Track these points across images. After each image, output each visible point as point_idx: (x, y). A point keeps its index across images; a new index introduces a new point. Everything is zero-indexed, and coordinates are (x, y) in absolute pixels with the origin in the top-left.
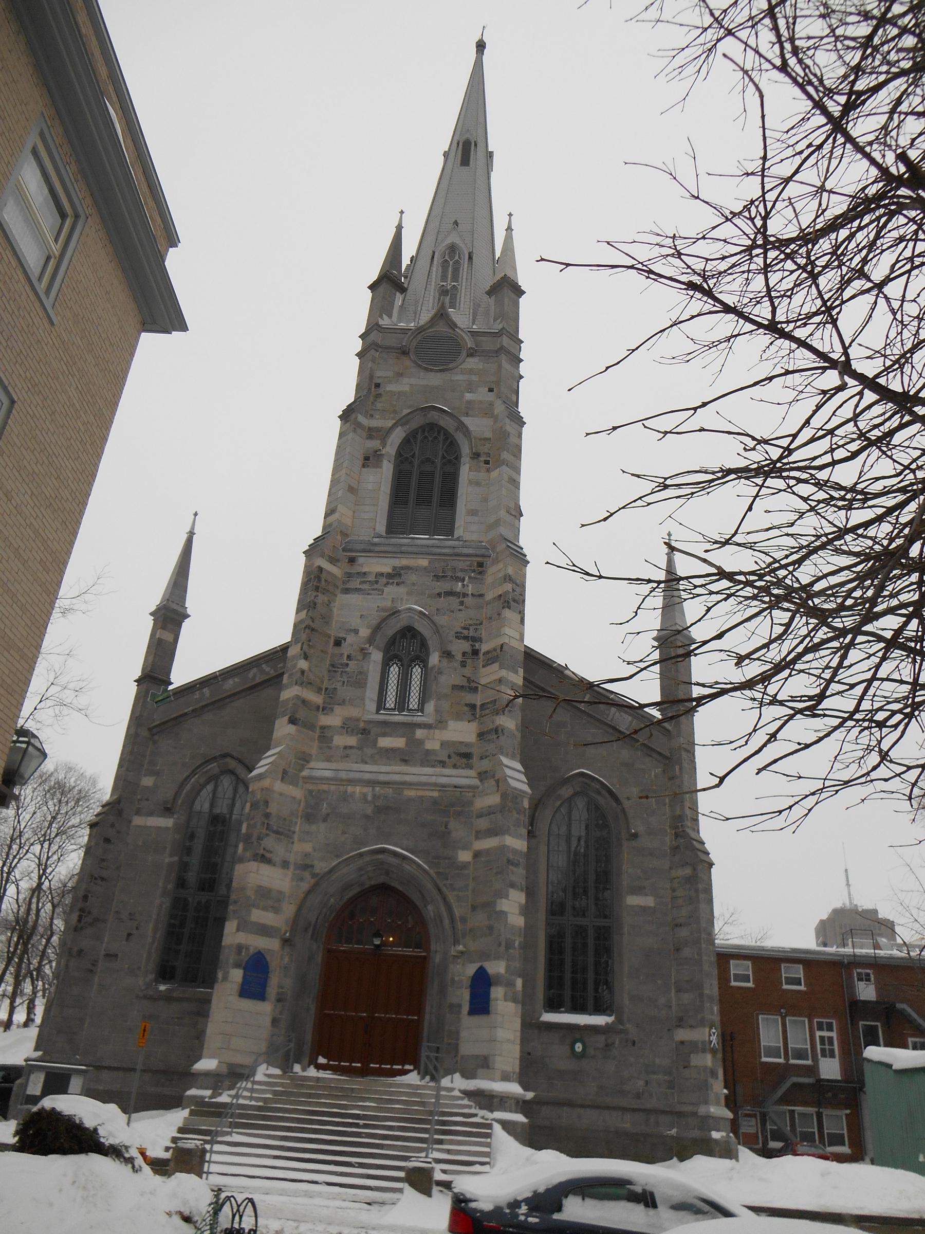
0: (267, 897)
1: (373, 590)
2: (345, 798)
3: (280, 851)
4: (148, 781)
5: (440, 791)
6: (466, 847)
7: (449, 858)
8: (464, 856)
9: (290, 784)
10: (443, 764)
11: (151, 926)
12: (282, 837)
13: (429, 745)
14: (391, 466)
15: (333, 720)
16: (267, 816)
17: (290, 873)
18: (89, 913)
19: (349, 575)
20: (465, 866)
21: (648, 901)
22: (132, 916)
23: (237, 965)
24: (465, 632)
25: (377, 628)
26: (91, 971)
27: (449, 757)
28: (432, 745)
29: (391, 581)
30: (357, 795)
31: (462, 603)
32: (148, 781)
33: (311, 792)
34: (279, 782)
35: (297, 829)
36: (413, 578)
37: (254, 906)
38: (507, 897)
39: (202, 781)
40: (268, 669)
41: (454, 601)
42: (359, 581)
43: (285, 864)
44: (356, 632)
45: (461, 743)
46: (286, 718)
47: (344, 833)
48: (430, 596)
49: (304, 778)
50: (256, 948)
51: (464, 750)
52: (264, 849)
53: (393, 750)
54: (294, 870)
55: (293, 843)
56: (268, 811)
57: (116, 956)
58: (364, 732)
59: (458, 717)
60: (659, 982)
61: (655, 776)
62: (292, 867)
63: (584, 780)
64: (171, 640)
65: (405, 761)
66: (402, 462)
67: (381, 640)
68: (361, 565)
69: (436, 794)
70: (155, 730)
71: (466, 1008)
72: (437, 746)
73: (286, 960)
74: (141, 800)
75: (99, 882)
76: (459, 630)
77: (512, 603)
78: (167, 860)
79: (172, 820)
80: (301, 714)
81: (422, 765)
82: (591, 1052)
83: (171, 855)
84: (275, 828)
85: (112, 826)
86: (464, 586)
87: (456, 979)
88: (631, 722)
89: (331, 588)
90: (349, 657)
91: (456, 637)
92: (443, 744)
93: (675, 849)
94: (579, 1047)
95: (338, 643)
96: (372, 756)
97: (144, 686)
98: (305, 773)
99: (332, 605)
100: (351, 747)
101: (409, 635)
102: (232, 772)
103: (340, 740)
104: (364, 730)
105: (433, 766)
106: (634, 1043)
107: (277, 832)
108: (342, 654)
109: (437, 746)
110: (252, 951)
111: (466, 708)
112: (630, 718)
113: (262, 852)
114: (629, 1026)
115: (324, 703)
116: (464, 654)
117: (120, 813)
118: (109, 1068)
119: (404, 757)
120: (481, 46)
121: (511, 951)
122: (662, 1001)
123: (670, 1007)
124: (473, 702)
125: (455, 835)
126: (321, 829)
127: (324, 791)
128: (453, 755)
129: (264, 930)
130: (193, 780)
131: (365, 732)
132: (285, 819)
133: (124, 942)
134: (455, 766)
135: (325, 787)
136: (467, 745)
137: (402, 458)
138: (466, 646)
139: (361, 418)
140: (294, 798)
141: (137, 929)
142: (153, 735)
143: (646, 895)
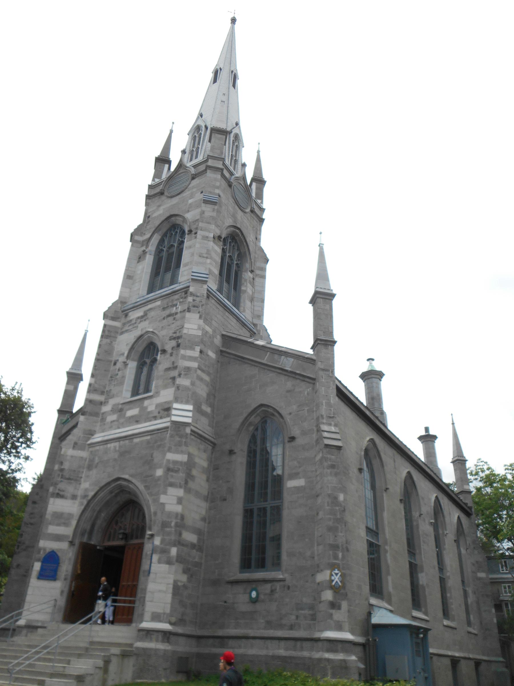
0: (61, 518)
3: (70, 489)
5: (150, 435)
7: (151, 476)
9: (79, 449)
10: (155, 418)
12: (72, 481)
13: (149, 409)
14: (152, 257)
15: (106, 409)
16: (62, 470)
17: (77, 502)
18: (24, 543)
19: (124, 324)
20: (159, 478)
25: (132, 348)
26: (25, 576)
31: (174, 319)
33: (91, 452)
35: (83, 476)
36: (152, 314)
37: (50, 524)
38: (165, 493)
41: (171, 318)
42: (128, 325)
43: (74, 497)
45: (165, 402)
47: (104, 472)
48: (160, 321)
49: (89, 445)
52: (59, 490)
53: (132, 417)
55: (80, 484)
56: (62, 467)
58: (121, 410)
59: (165, 387)
61: (308, 394)
62: (79, 498)
63: (263, 408)
65: (137, 422)
68: (130, 317)
76: (171, 335)
77: (192, 308)
81: (145, 422)
82: (262, 597)
84: (67, 477)
85: (37, 494)
86: (176, 308)
88: (293, 362)
89: (113, 334)
90: (119, 370)
92: (157, 406)
94: (254, 594)
96: (123, 423)
98: (89, 442)
99: (114, 343)
100: (114, 421)
101: (152, 347)
103: (110, 418)
105: (150, 421)
106: (289, 588)
107: (69, 479)
108: (116, 369)
110: (48, 551)
111: (170, 380)
112: (292, 360)
113: (57, 491)
115: (105, 399)
119: (136, 420)
120: (234, 21)
121: (168, 529)
122: (308, 553)
123: (314, 557)
125: (156, 461)
126: (94, 472)
129: (58, 538)
131: (120, 410)
132: (74, 471)
134: (161, 418)
137: (159, 251)
138: (173, 343)
139: (137, 238)
140: (82, 458)
143: (300, 478)
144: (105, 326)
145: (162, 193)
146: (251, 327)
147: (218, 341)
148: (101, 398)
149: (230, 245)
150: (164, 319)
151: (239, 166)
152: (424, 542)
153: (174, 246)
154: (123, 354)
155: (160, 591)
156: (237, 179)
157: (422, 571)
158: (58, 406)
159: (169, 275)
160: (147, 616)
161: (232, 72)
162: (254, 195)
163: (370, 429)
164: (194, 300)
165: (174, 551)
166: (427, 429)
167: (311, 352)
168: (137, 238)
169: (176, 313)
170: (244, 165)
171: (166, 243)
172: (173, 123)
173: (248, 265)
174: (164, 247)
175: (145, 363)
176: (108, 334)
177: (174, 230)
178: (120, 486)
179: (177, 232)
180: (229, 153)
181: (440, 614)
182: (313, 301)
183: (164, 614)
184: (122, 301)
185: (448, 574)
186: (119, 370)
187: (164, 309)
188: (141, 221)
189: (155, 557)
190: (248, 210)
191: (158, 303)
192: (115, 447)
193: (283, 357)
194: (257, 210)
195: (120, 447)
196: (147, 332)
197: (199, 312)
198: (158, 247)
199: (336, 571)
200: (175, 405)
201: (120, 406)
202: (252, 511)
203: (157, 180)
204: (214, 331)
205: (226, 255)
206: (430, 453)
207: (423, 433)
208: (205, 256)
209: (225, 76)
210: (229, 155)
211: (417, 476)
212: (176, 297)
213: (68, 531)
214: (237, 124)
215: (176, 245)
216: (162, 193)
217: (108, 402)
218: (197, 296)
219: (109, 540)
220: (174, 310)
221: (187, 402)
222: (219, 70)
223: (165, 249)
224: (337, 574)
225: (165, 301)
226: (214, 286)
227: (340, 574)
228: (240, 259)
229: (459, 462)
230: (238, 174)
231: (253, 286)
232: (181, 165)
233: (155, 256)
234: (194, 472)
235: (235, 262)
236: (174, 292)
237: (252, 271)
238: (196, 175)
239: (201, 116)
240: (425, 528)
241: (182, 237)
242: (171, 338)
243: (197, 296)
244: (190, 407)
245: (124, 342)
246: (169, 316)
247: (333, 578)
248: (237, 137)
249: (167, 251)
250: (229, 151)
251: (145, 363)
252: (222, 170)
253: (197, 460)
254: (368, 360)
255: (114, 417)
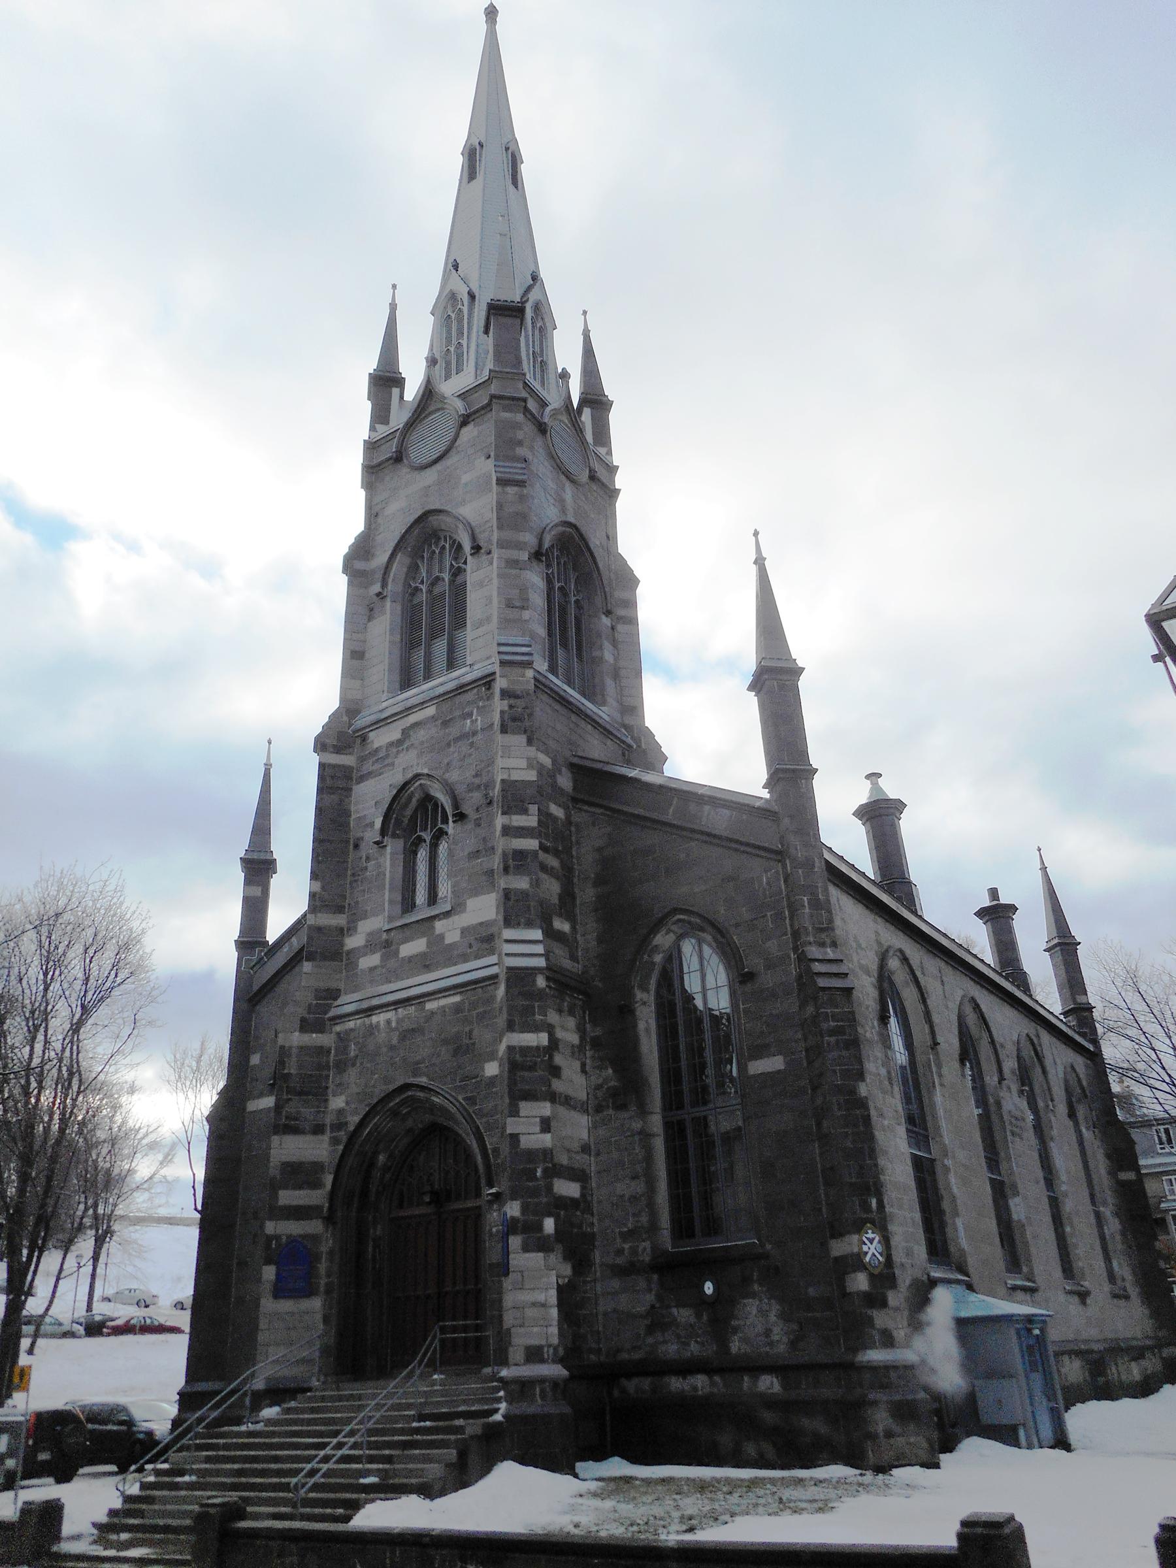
0: (300, 1174)
2: (371, 1030)
5: (461, 993)
6: (492, 1056)
10: (465, 958)
15: (353, 942)
17: (326, 1138)
19: (362, 759)
20: (492, 1080)
21: (773, 1064)
28: (452, 937)
30: (382, 1023)
34: (297, 1034)
36: (421, 735)
38: (515, 1113)
43: (318, 1130)
45: (481, 924)
49: (331, 1019)
50: (289, 1236)
58: (387, 944)
59: (476, 892)
61: (768, 883)
65: (428, 968)
69: (457, 999)
81: (446, 966)
86: (472, 722)
89: (340, 783)
90: (368, 858)
92: (464, 931)
98: (331, 1014)
100: (375, 967)
103: (367, 962)
104: (387, 941)
115: (348, 923)
119: (424, 963)
127: (351, 1030)
131: (385, 944)
135: (351, 1025)
138: (477, 797)
144: (322, 766)
145: (398, 458)
146: (623, 733)
147: (565, 781)
148: (340, 920)
149: (558, 564)
150: (449, 745)
151: (552, 377)
152: (1013, 1134)
153: (443, 580)
154: (372, 824)
155: (534, 1304)
156: (555, 412)
157: (1017, 1194)
158: (236, 934)
159: (440, 647)
160: (516, 1353)
161: (507, 149)
162: (589, 437)
163: (892, 928)
164: (511, 707)
165: (549, 1225)
166: (994, 893)
167: (765, 794)
168: (359, 565)
169: (475, 733)
170: (565, 375)
171: (424, 574)
172: (394, 287)
173: (598, 600)
174: (422, 582)
175: (420, 840)
176: (334, 787)
177: (437, 546)
178: (412, 1098)
179: (443, 548)
180: (528, 351)
181: (1058, 1273)
182: (757, 685)
183: (549, 1346)
184: (349, 708)
185: (1064, 1188)
186: (368, 858)
187: (445, 724)
188: (358, 525)
189: (515, 1242)
190: (584, 477)
191: (431, 711)
192: (388, 1022)
193: (707, 808)
194: (601, 473)
195: (399, 1021)
196: (417, 776)
197: (525, 732)
198: (407, 585)
199: (870, 1235)
200: (508, 934)
201: (384, 936)
202: (681, 1125)
203: (383, 430)
204: (554, 762)
205: (553, 587)
206: (1006, 945)
207: (987, 903)
208: (518, 604)
209: (492, 160)
210: (528, 355)
211: (987, 1002)
212: (470, 696)
213: (316, 1197)
214: (535, 278)
215: (446, 576)
216: (398, 458)
217: (355, 929)
218: (517, 697)
219: (401, 1206)
221: (529, 924)
222: (478, 147)
223: (424, 588)
224: (871, 1241)
225: (446, 707)
226: (542, 666)
227: (877, 1239)
228: (582, 587)
229: (1065, 948)
230: (554, 401)
231: (615, 643)
232: (428, 393)
233: (403, 605)
234: (558, 1059)
235: (573, 599)
236: (461, 689)
237: (608, 613)
238: (468, 416)
239: (456, 267)
240: (1013, 1102)
241: (456, 559)
242: (471, 788)
243: (517, 697)
244: (537, 934)
245: (370, 799)
247: (865, 1248)
248: (541, 309)
249: (430, 592)
250: (527, 345)
251: (420, 840)
252: (525, 400)
253: (560, 1034)
254: (868, 777)
255: (373, 960)
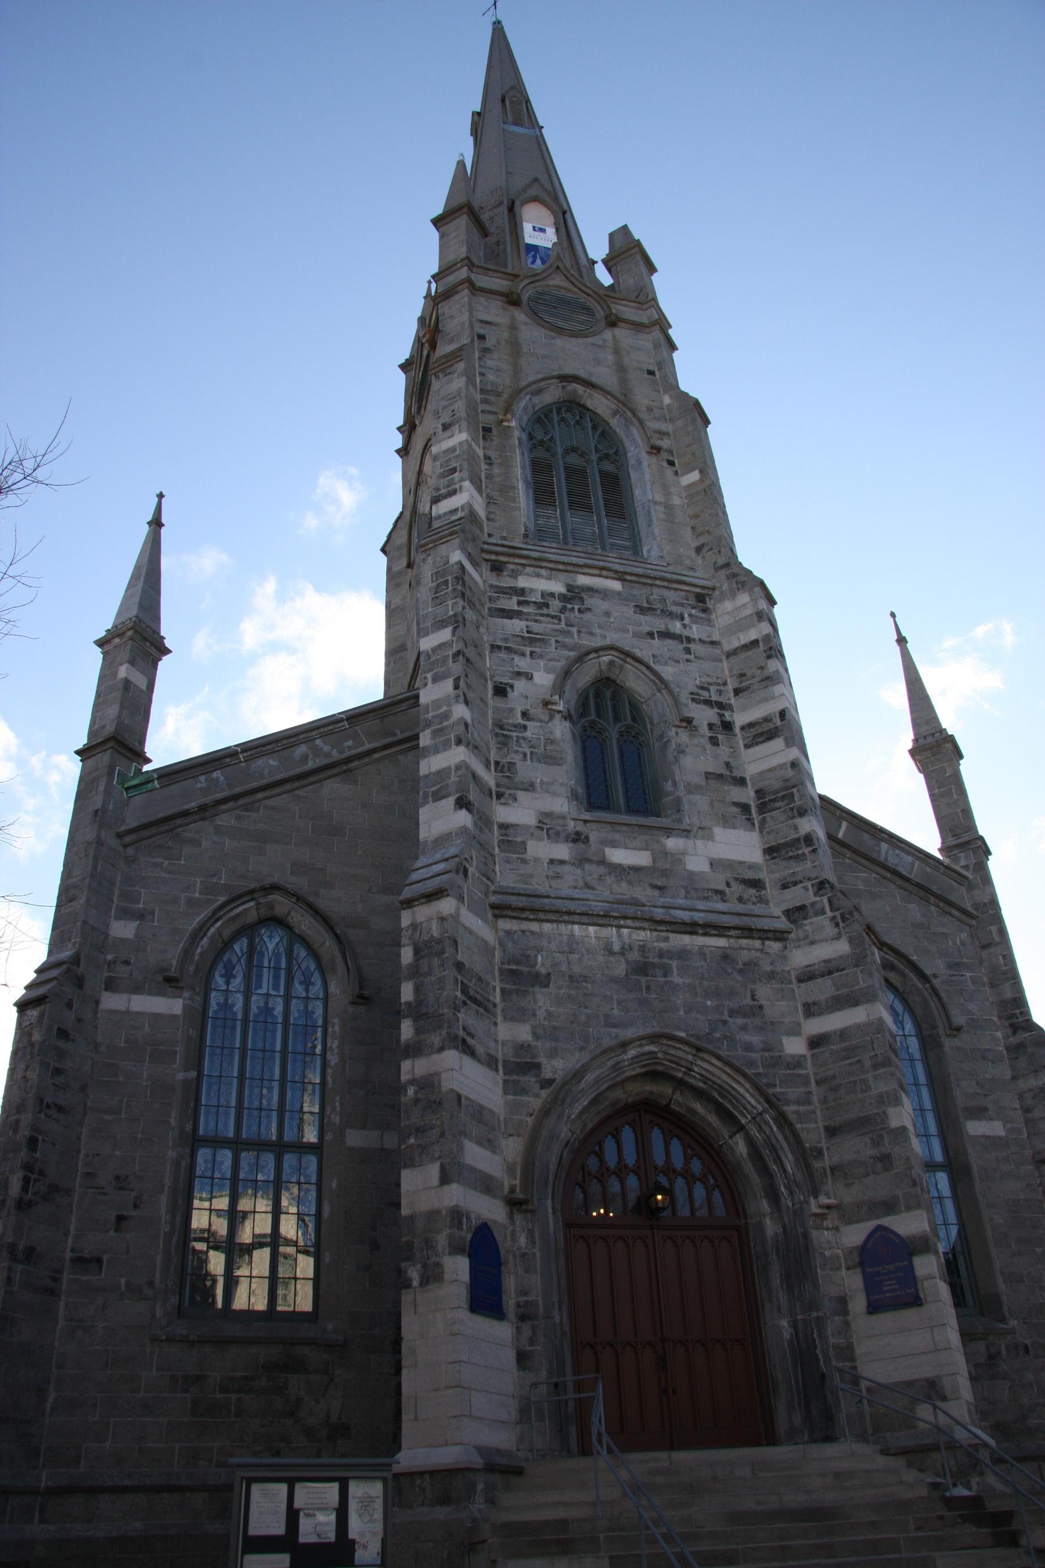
1: (542, 615)
4: (123, 930)
6: (795, 1031)
8: (794, 1046)
11: (164, 1200)
18: (41, 1173)
20: (798, 1062)
21: (996, 1128)
22: (121, 1182)
23: (456, 1249)
24: (705, 693)
27: (728, 885)
29: (569, 606)
32: (123, 930)
39: (227, 933)
40: (326, 748)
41: (676, 647)
42: (515, 599)
43: (491, 1062)
44: (529, 677)
45: (741, 863)
46: (451, 801)
48: (636, 635)
51: (749, 875)
54: (505, 1074)
57: (99, 1261)
59: (727, 822)
60: (1038, 1250)
61: (963, 943)
64: (144, 688)
66: (534, 447)
67: (571, 695)
70: (128, 839)
71: (858, 1304)
72: (703, 867)
73: (523, 1240)
74: (115, 962)
75: (54, 1113)
76: (696, 690)
78: (180, 1076)
79: (181, 1001)
80: (473, 796)
83: (186, 1069)
85: (69, 1005)
87: (827, 1253)
90: (525, 714)
91: (693, 700)
92: (713, 863)
93: (1015, 1050)
95: (501, 691)
97: (104, 758)
100: (562, 862)
102: (280, 922)
109: (703, 867)
111: (735, 809)
114: (1013, 1323)
115: (498, 785)
116: (711, 726)
117: (79, 982)
118: (115, 1490)
124: (744, 801)
128: (733, 883)
129: (486, 1184)
130: (212, 930)
133: (112, 1233)
136: (752, 866)
141: (136, 1206)
142: (125, 846)
220: (677, 627)
246: (666, 635)
